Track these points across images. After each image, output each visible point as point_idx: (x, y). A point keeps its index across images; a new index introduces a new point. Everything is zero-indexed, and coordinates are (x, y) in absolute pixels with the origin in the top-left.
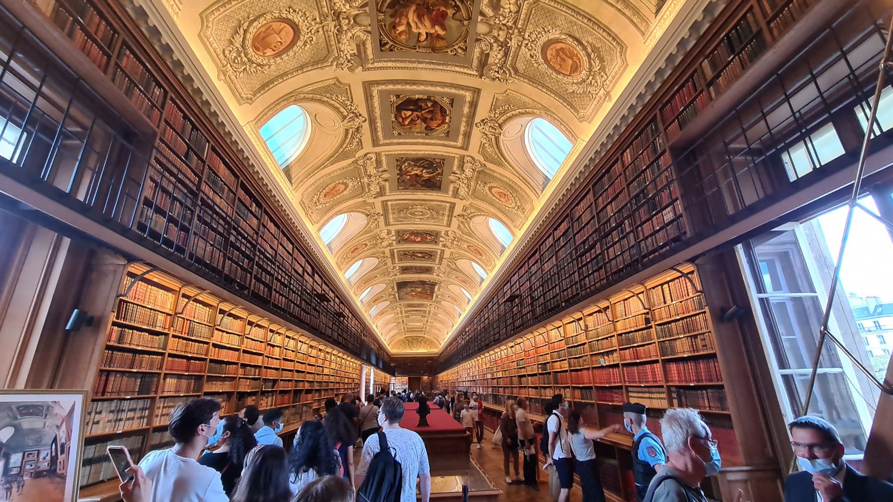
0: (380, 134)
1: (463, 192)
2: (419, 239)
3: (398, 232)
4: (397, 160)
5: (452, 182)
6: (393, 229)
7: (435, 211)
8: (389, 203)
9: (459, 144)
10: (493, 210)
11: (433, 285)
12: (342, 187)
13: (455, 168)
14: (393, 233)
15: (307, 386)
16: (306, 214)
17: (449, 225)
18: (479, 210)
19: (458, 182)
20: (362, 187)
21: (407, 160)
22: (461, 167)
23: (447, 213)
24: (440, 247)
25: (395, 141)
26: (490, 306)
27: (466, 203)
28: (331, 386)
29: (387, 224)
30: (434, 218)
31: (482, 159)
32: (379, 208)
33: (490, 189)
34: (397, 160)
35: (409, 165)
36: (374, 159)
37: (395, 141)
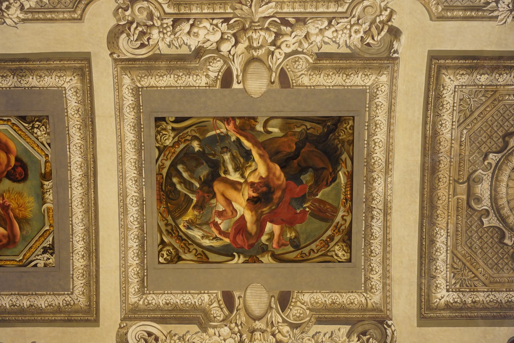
0: (42, 302)
8: (443, 295)
9: (70, 83)
25: (79, 262)
37: (79, 262)
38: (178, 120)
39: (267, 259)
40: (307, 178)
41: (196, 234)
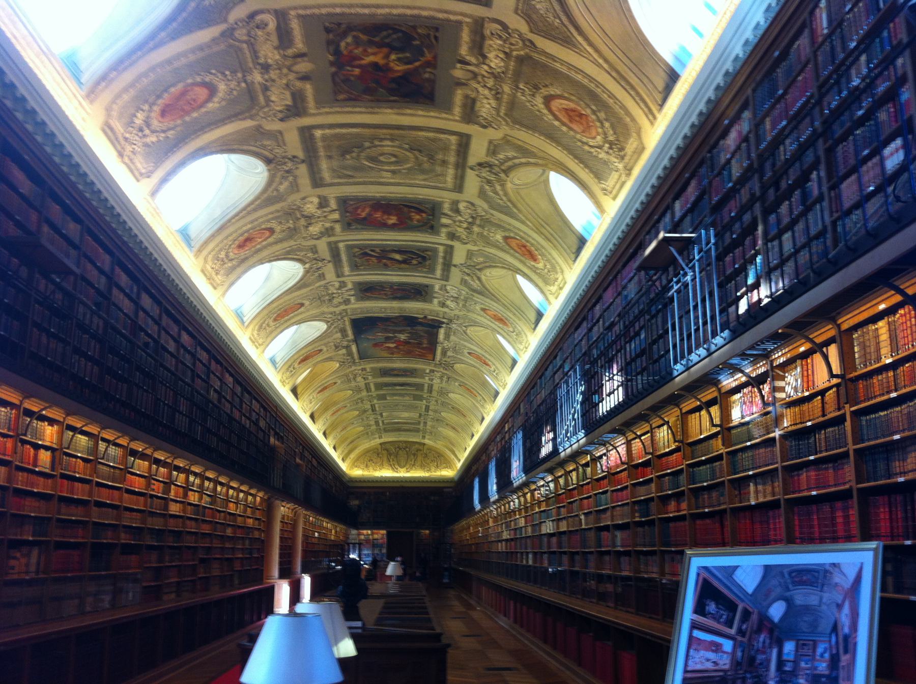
1: (486, 107)
2: (393, 220)
3: (343, 202)
4: (328, 30)
5: (460, 84)
6: (332, 193)
7: (424, 152)
8: (318, 133)
10: (556, 152)
11: (433, 326)
12: (202, 93)
13: (464, 51)
14: (333, 205)
15: (124, 538)
16: (121, 155)
17: (459, 187)
18: (524, 151)
19: (474, 85)
20: (252, 97)
21: (350, 29)
22: (478, 46)
23: (452, 159)
24: (442, 238)
26: (549, 373)
27: (495, 134)
28: (189, 542)
29: (317, 182)
30: (423, 172)
31: (523, 27)
32: (294, 145)
33: (548, 100)
34: (328, 30)
35: (357, 42)
36: (272, 25)
38: (436, 38)
39: (333, 69)
40: (394, 85)
41: (349, 39)
